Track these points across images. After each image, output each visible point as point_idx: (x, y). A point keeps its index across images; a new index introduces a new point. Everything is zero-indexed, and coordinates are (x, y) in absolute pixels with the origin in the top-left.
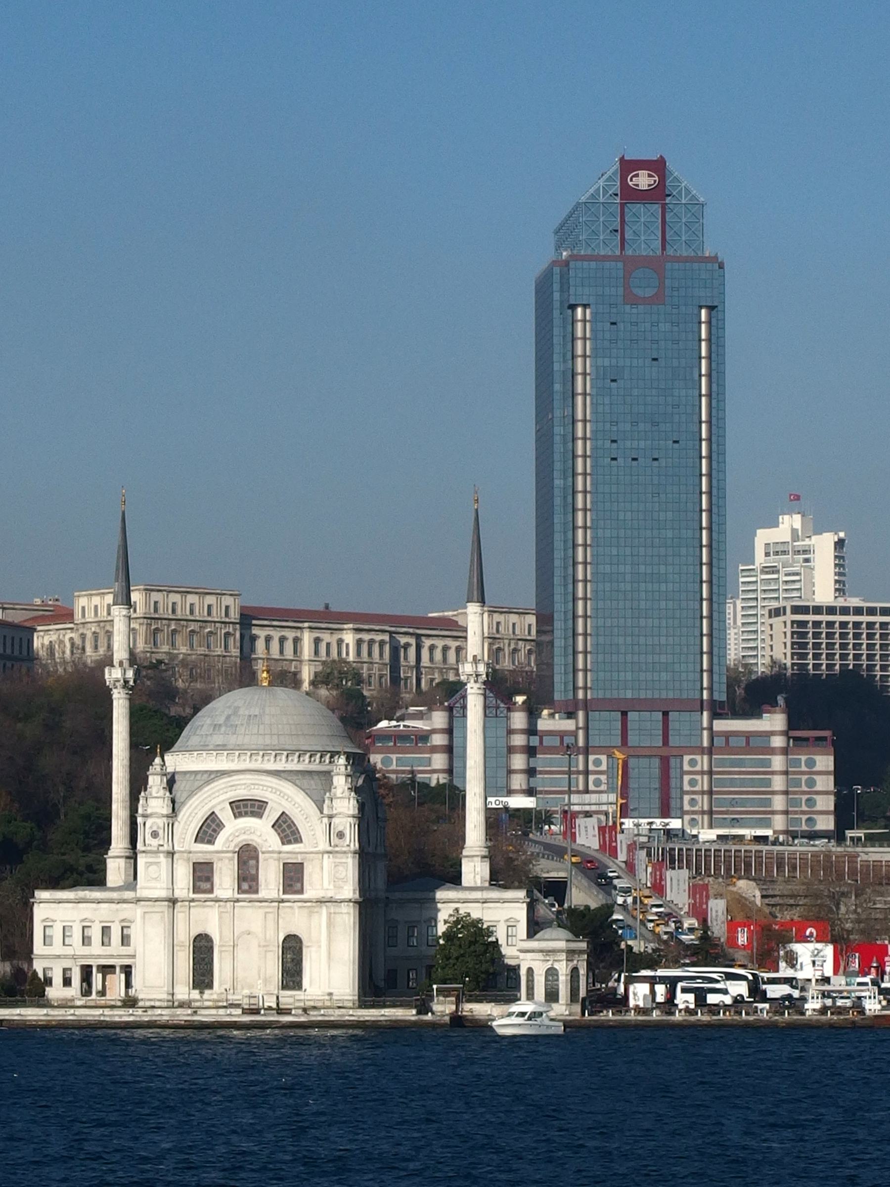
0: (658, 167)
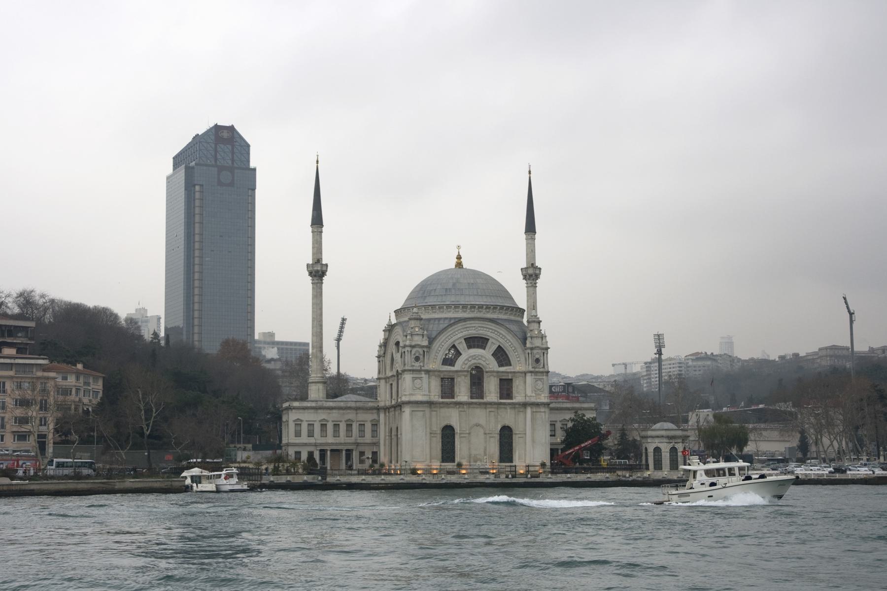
0: (232, 129)
